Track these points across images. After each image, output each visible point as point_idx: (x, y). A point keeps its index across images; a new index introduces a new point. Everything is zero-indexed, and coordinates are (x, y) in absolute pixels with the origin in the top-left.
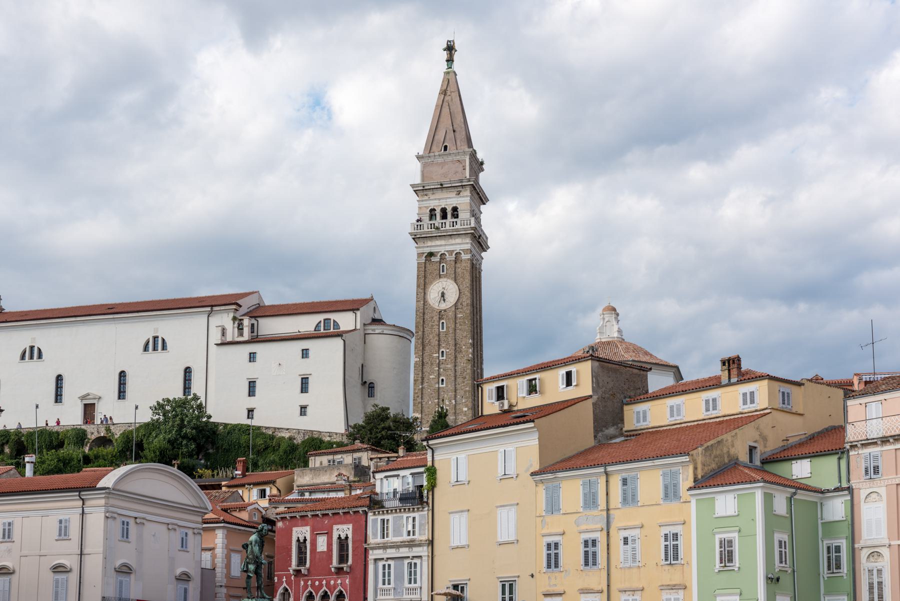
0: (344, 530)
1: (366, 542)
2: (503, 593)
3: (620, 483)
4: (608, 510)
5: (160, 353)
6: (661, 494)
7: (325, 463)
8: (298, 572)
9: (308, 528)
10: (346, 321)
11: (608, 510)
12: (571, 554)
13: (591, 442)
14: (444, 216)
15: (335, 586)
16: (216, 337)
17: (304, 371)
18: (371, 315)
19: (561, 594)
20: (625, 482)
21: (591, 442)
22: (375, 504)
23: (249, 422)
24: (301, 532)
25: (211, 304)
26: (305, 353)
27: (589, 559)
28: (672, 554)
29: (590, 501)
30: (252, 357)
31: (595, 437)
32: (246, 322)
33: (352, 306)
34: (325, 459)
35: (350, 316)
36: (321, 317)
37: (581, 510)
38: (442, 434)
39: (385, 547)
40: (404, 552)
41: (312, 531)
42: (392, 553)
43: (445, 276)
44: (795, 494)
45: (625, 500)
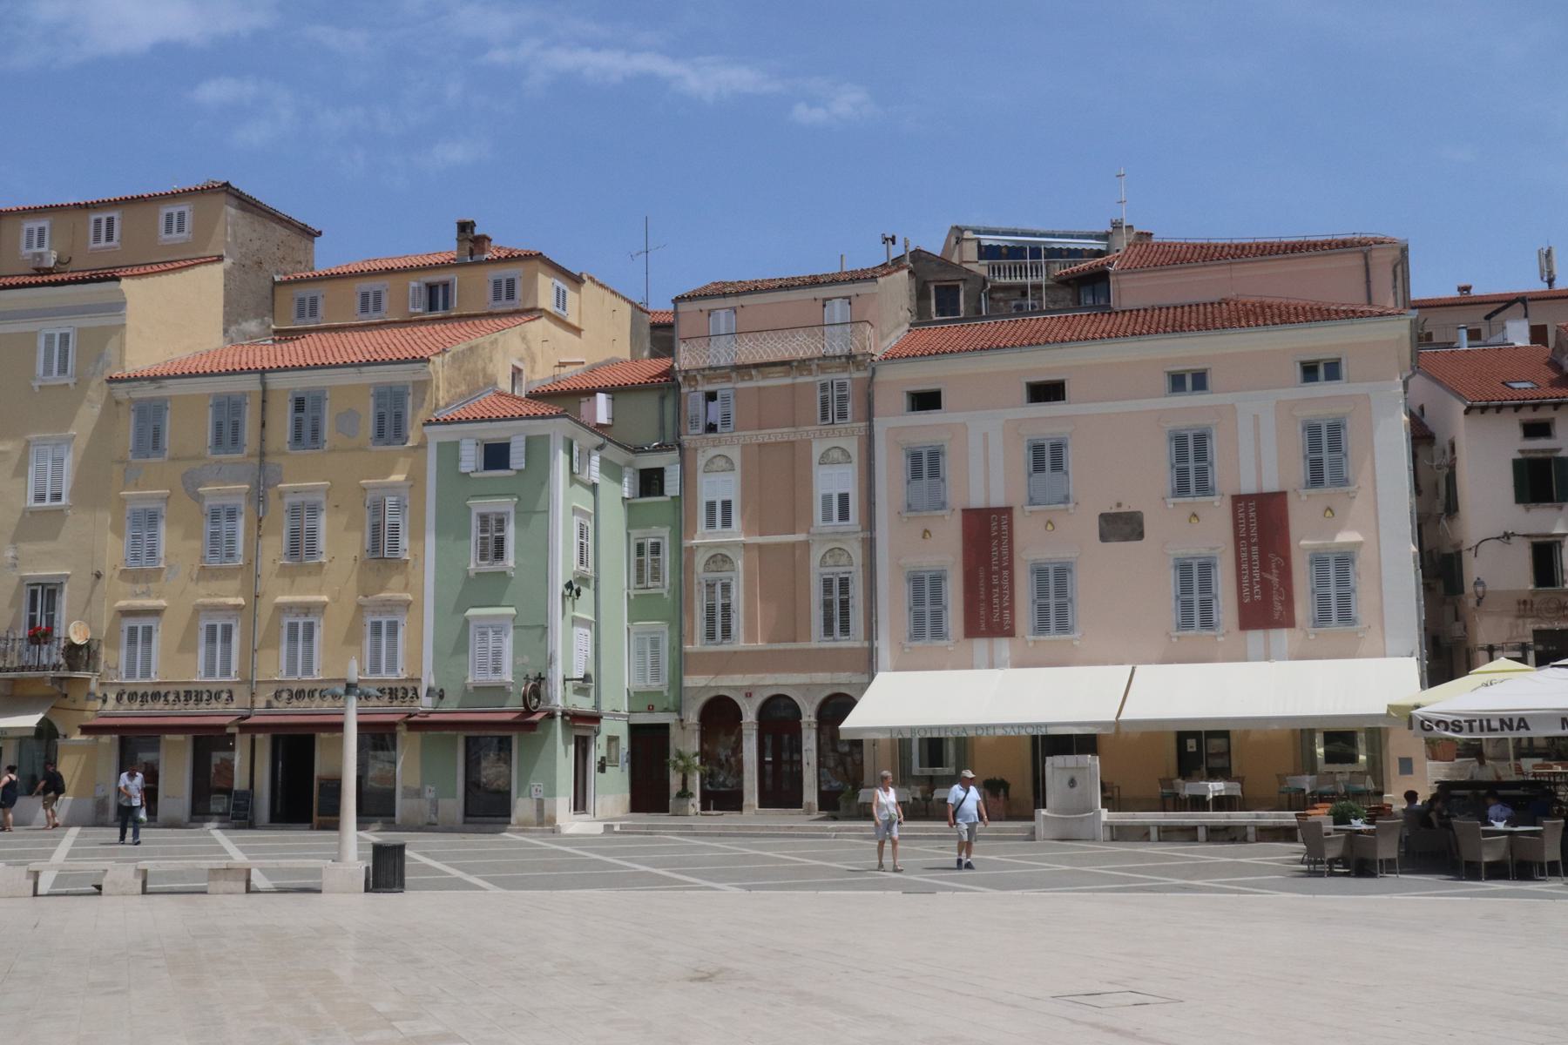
2: (33, 607)
3: (290, 407)
20: (299, 404)
31: (226, 331)
37: (209, 452)
45: (297, 437)
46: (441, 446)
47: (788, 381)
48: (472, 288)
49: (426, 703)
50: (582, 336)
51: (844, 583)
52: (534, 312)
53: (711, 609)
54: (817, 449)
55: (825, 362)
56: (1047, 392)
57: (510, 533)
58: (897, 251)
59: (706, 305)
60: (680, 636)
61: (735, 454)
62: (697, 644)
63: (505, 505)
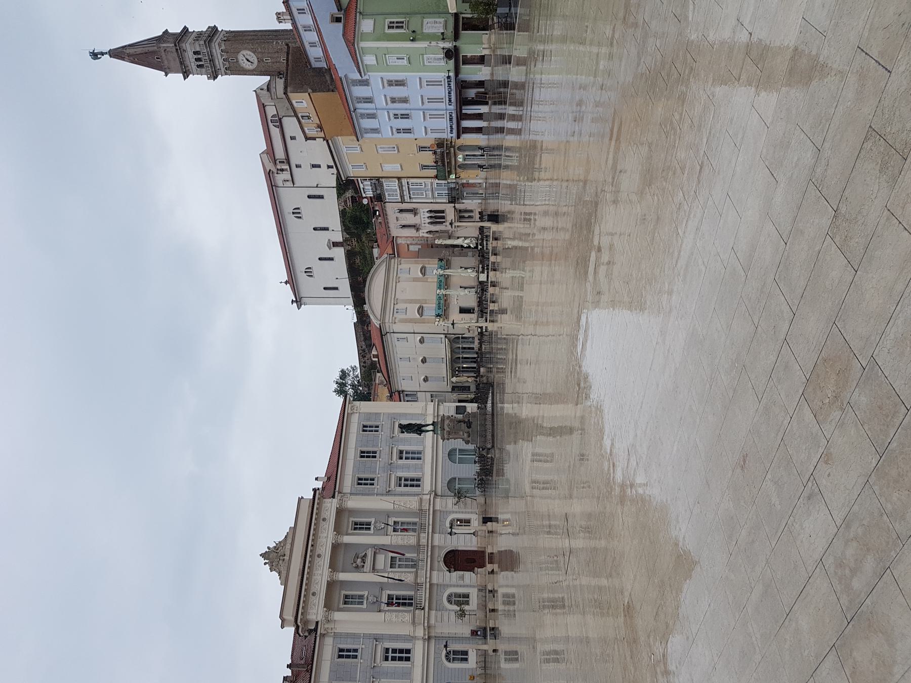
5: (303, 211)
6: (366, 87)
10: (271, 111)
14: (197, 60)
16: (290, 184)
18: (265, 92)
21: (336, 95)
25: (272, 187)
29: (373, 116)
30: (298, 166)
32: (279, 167)
33: (262, 107)
35: (267, 108)
36: (271, 125)
39: (402, 196)
42: (406, 193)
44: (360, 13)
49: (452, 74)
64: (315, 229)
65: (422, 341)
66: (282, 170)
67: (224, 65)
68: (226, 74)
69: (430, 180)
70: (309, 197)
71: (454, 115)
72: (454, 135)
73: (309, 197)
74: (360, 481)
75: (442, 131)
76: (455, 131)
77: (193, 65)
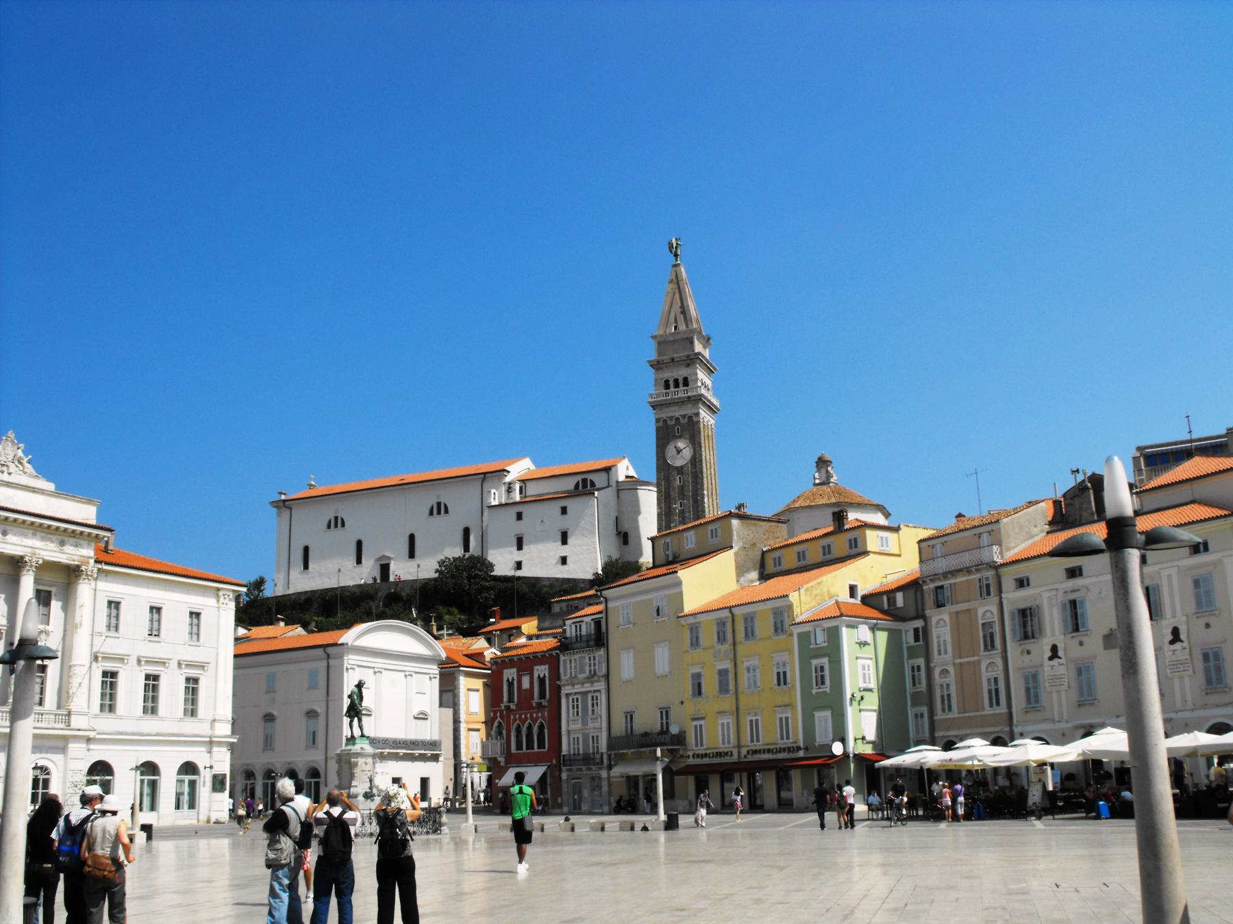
0: (542, 670)
1: (559, 678)
4: (734, 644)
6: (772, 630)
7: (565, 609)
8: (508, 708)
9: (515, 670)
11: (734, 644)
12: (710, 684)
13: (732, 586)
15: (537, 718)
17: (564, 527)
19: (703, 718)
20: (746, 620)
21: (732, 586)
22: (565, 646)
23: (519, 573)
24: (510, 674)
26: (564, 511)
27: (723, 688)
28: (782, 679)
29: (721, 638)
30: (519, 516)
34: (564, 605)
35: (604, 475)
38: (626, 581)
39: (573, 682)
40: (587, 687)
41: (518, 672)
43: (680, 437)
45: (746, 635)
46: (800, 635)
47: (965, 579)
48: (840, 544)
49: (801, 754)
50: (890, 561)
51: (996, 679)
52: (865, 553)
53: (942, 697)
54: (980, 611)
55: (978, 567)
56: (1074, 573)
57: (827, 673)
58: (1080, 478)
59: (931, 543)
60: (932, 713)
61: (946, 617)
62: (940, 715)
63: (825, 661)
64: (412, 538)
65: (312, 714)
66: (510, 489)
67: (671, 418)
68: (658, 420)
69: (604, 725)
70: (467, 532)
71: (727, 759)
72: (691, 761)
73: (467, 532)
74: (114, 605)
75: (699, 740)
76: (698, 761)
77: (670, 374)
